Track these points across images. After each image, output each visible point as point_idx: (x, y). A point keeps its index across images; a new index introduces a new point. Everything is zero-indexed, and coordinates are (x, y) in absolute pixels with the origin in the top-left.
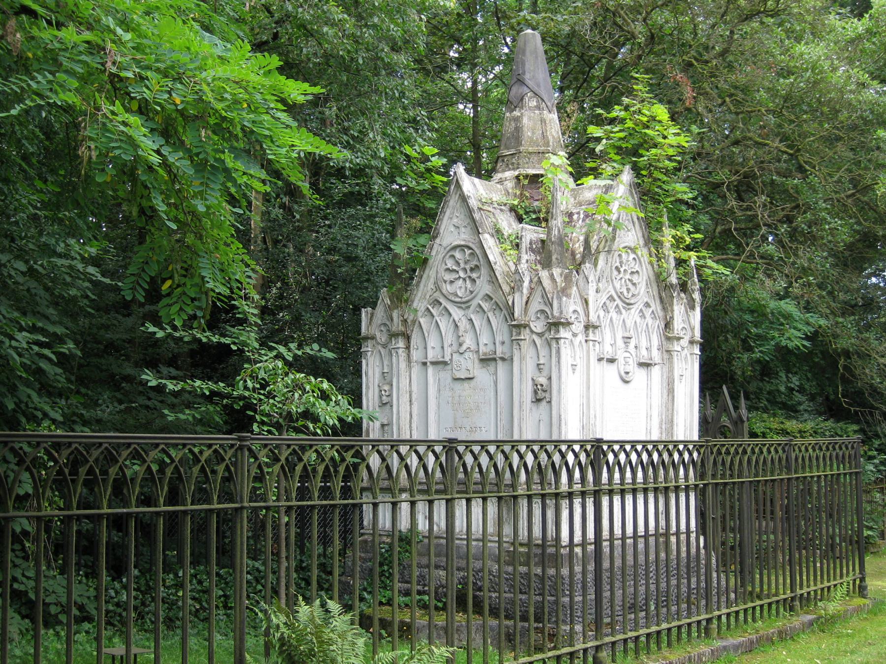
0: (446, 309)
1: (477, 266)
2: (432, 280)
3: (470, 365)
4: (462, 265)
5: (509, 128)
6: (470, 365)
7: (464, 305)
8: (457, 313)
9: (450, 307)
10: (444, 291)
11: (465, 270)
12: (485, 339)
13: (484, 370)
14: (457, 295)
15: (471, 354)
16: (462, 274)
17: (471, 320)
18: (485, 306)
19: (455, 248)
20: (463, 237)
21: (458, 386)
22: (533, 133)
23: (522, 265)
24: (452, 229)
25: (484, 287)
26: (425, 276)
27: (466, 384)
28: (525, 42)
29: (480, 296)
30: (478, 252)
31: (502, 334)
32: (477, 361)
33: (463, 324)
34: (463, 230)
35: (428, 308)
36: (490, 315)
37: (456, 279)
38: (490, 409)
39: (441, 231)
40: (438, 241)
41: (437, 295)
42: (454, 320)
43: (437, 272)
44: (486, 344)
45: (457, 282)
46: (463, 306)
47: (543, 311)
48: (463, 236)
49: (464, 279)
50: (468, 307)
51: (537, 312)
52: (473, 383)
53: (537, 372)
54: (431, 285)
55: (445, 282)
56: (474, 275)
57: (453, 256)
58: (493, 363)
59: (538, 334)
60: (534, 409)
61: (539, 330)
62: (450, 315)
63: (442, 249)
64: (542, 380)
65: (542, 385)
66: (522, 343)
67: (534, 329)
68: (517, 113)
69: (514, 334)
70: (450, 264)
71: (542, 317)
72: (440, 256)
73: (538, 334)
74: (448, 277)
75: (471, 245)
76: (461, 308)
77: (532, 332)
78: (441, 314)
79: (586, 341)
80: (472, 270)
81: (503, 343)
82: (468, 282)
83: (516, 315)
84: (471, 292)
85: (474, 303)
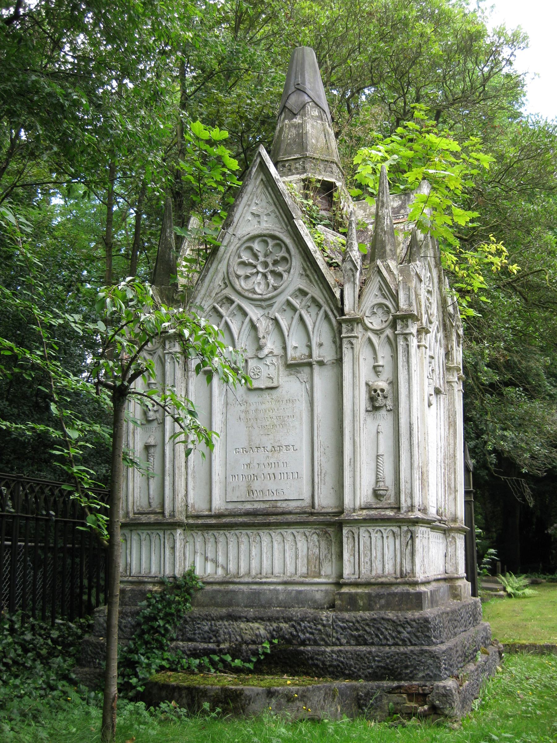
0: (240, 308)
1: (284, 259)
2: (220, 276)
3: (272, 371)
4: (261, 259)
5: (289, 134)
6: (272, 371)
7: (265, 303)
8: (254, 313)
9: (246, 306)
10: (238, 287)
11: (266, 265)
12: (295, 341)
13: (293, 378)
14: (255, 292)
15: (275, 360)
16: (260, 269)
17: (276, 320)
18: (296, 302)
19: (253, 238)
20: (269, 224)
21: (253, 398)
22: (317, 141)
23: (354, 253)
24: (250, 218)
25: (294, 279)
26: (212, 270)
27: (266, 396)
28: (303, 54)
29: (292, 289)
30: (288, 241)
31: (321, 334)
32: (282, 368)
33: (263, 325)
34: (265, 218)
35: (214, 308)
36: (304, 313)
37: (252, 274)
38: (301, 424)
39: (236, 220)
40: (230, 230)
41: (228, 292)
42: (251, 321)
43: (228, 265)
44: (296, 347)
45: (253, 279)
46: (263, 304)
47: (380, 305)
48: (264, 225)
49: (265, 276)
50: (271, 306)
51: (373, 307)
52: (275, 393)
53: (373, 374)
54: (219, 281)
55: (238, 277)
56: (280, 269)
57: (250, 249)
58: (307, 370)
59: (375, 332)
60: (369, 420)
61: (376, 327)
62: (245, 314)
63: (236, 240)
64: (382, 384)
65: (382, 390)
66: (354, 341)
67: (370, 325)
68: (297, 120)
69: (344, 330)
70: (246, 257)
71: (380, 312)
72: (233, 248)
73: (375, 332)
74: (241, 272)
75: (277, 234)
76: (261, 307)
77: (366, 329)
78: (233, 315)
79: (419, 347)
80: (276, 263)
81: (321, 345)
82: (269, 277)
83: (346, 309)
84: (275, 288)
85: (280, 300)
